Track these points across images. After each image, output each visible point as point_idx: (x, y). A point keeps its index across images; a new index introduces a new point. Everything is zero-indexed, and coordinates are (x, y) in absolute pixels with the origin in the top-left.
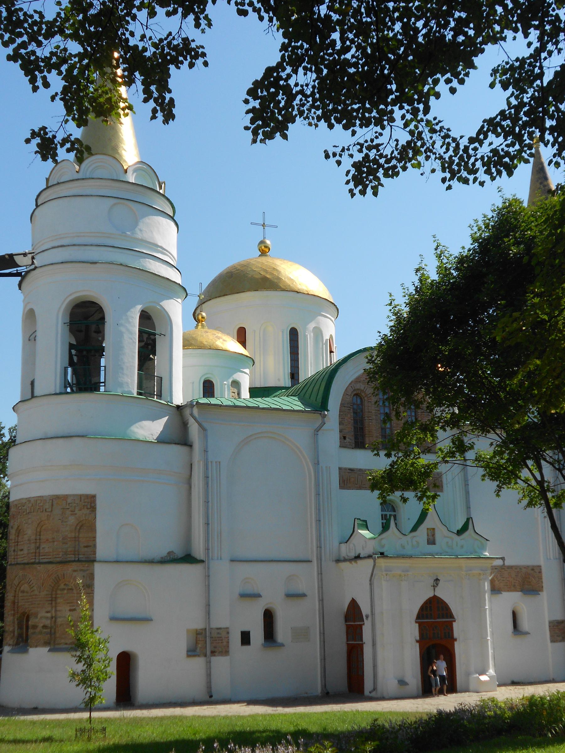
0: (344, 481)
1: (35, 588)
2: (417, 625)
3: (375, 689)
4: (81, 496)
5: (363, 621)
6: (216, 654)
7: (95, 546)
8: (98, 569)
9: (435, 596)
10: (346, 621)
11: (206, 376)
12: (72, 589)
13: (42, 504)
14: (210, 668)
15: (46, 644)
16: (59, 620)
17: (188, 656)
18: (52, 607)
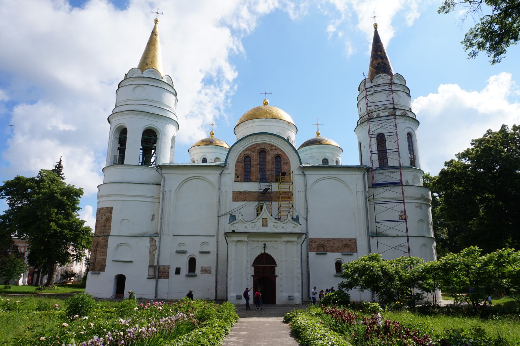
0: (235, 198)
2: (253, 267)
4: (108, 208)
6: (162, 278)
8: (110, 238)
9: (265, 253)
17: (148, 278)
18: (94, 254)
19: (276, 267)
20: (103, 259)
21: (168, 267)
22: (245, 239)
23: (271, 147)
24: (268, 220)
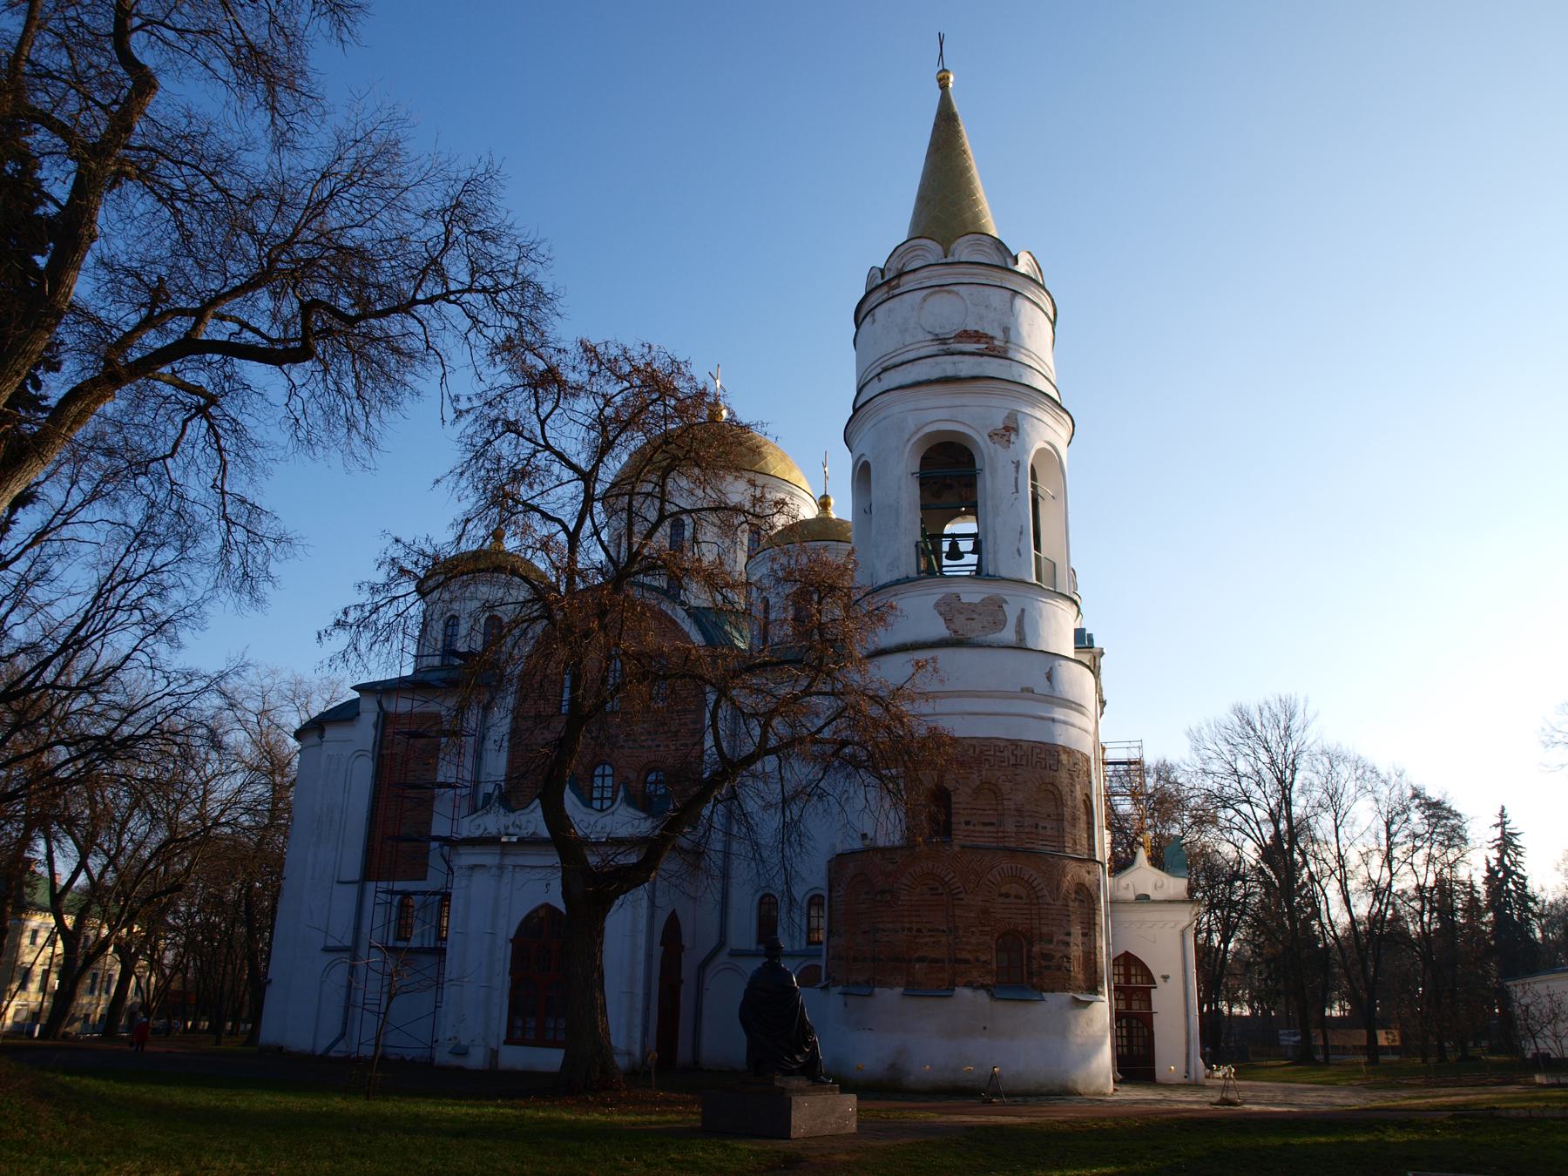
1: (1045, 892)
12: (1083, 901)
13: (1043, 756)
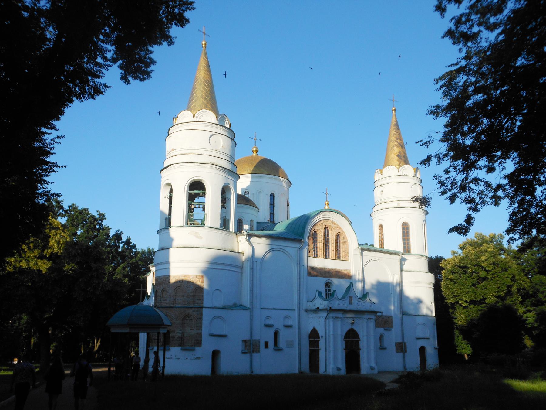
3: (326, 371)
5: (319, 338)
7: (203, 300)
8: (205, 311)
10: (309, 339)
11: (240, 217)
12: (192, 320)
14: (252, 359)
15: (180, 345)
16: (186, 334)
17: (243, 353)
19: (360, 342)
20: (197, 333)
21: (259, 341)
22: (340, 315)
23: (334, 225)
24: (353, 298)
